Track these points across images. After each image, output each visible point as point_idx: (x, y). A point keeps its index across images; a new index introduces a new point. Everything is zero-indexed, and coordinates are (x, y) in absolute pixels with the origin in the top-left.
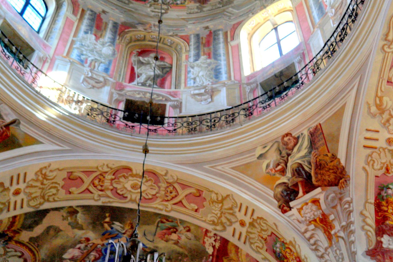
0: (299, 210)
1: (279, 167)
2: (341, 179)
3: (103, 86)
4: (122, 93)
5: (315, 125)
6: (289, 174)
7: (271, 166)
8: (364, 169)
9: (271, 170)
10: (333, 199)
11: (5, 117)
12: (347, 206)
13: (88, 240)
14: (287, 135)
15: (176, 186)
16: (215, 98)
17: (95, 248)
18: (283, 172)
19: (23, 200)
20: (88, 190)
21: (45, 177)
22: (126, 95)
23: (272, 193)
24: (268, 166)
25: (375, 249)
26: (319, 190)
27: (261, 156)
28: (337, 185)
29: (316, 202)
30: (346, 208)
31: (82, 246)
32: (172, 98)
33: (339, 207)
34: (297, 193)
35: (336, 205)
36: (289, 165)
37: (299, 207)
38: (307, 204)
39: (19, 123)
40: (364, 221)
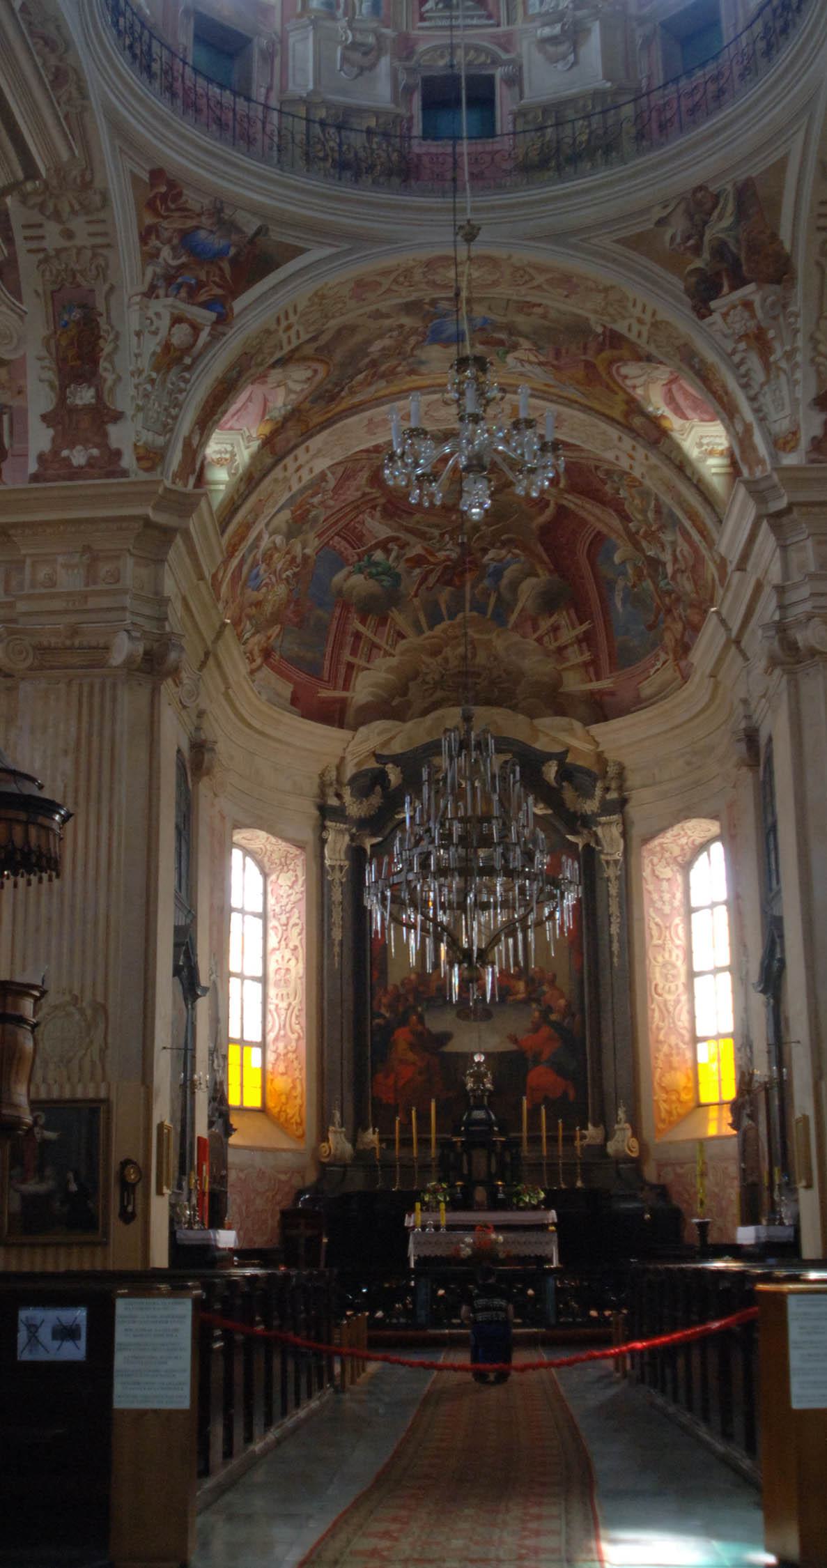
0: (725, 316)
1: (691, 242)
2: (785, 274)
3: (378, 58)
4: (412, 63)
5: (744, 177)
6: (706, 255)
7: (678, 240)
9: (679, 245)
10: (773, 305)
11: (245, 229)
12: (792, 320)
13: (402, 326)
14: (701, 188)
15: (531, 271)
16: (583, 51)
17: (414, 331)
18: (697, 250)
19: (298, 331)
20: (389, 290)
21: (323, 297)
22: (420, 66)
24: (673, 238)
26: (751, 287)
27: (661, 222)
28: (778, 282)
29: (748, 305)
30: (790, 324)
31: (395, 333)
32: (504, 56)
33: (781, 319)
34: (721, 286)
35: (778, 315)
36: (707, 238)
37: (724, 310)
38: (734, 307)
39: (267, 229)
40: (815, 349)
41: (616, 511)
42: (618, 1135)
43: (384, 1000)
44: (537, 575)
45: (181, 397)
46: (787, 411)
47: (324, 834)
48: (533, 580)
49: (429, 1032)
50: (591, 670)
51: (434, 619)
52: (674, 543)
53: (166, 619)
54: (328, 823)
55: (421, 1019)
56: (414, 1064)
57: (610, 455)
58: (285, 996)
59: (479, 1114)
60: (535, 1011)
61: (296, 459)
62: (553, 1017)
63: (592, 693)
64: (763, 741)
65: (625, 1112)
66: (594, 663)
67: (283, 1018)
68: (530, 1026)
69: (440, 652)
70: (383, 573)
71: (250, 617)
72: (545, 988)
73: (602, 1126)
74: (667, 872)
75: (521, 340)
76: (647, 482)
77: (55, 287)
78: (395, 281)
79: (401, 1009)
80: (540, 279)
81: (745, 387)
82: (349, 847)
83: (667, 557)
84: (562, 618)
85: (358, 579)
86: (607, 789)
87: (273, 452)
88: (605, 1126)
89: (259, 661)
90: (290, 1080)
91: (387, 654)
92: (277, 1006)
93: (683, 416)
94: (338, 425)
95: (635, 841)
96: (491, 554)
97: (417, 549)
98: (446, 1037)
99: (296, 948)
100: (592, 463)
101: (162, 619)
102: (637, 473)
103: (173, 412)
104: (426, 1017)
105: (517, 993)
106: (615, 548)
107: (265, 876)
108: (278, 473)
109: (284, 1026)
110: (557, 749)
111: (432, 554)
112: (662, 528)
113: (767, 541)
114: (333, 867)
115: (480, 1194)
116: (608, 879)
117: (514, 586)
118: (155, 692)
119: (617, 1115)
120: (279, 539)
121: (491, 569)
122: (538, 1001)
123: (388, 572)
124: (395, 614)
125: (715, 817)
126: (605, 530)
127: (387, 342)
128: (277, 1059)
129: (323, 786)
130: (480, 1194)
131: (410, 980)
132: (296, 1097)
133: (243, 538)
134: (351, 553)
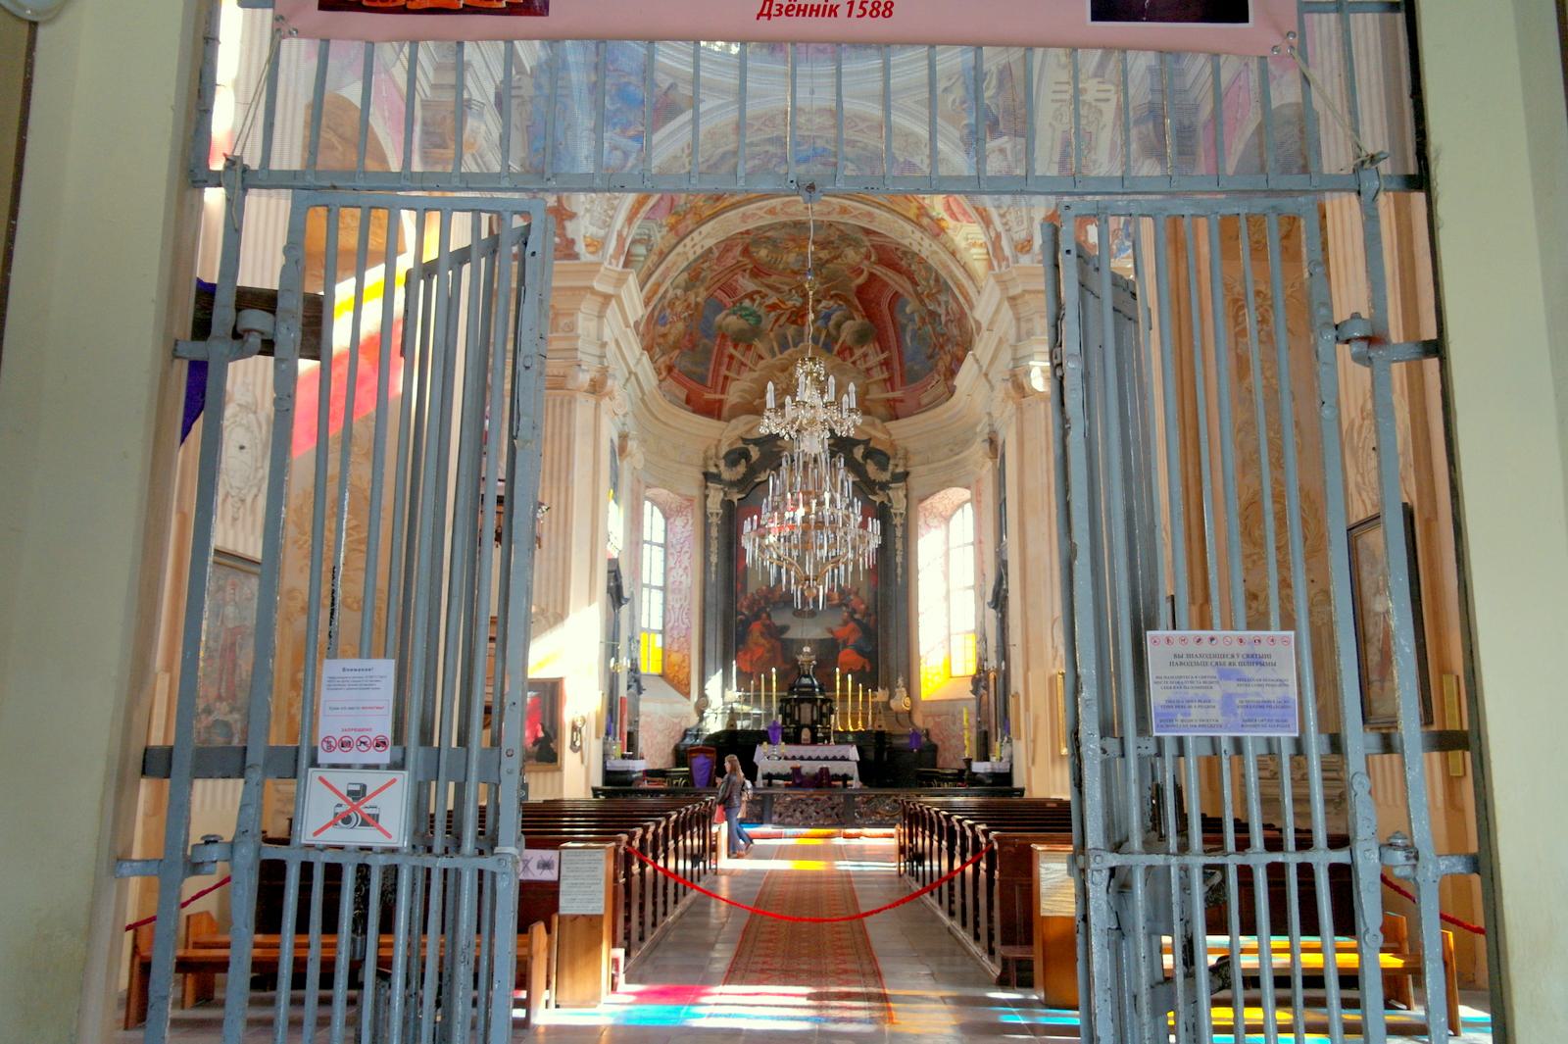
8: (1050, 124)
20: (759, 130)
23: (957, 134)
24: (954, 101)
25: (1053, 215)
26: (1006, 138)
31: (762, 157)
41: (909, 278)
44: (854, 319)
45: (616, 202)
46: (1025, 225)
47: (707, 492)
48: (850, 323)
50: (888, 384)
51: (784, 346)
52: (947, 302)
53: (605, 357)
54: (709, 484)
56: (763, 645)
57: (906, 242)
59: (806, 681)
60: (844, 613)
61: (692, 239)
62: (857, 616)
63: (888, 400)
64: (1000, 442)
66: (890, 380)
68: (840, 622)
69: (787, 369)
70: (750, 315)
71: (659, 345)
72: (852, 597)
74: (934, 522)
75: (849, 164)
76: (930, 261)
77: (529, 123)
78: (764, 124)
80: (862, 125)
81: (998, 207)
82: (723, 501)
83: (941, 311)
84: (870, 348)
85: (732, 319)
86: (897, 466)
87: (677, 234)
89: (664, 374)
91: (751, 370)
93: (957, 220)
94: (722, 217)
95: (913, 501)
96: (824, 303)
97: (773, 299)
98: (785, 629)
99: (686, 568)
100: (893, 246)
101: (602, 357)
102: (924, 255)
103: (610, 213)
104: (772, 615)
106: (907, 303)
107: (666, 518)
108: (680, 249)
110: (865, 438)
111: (783, 303)
112: (939, 292)
113: (1007, 312)
114: (712, 514)
115: (806, 734)
116: (896, 526)
117: (838, 326)
118: (597, 406)
120: (679, 292)
121: (823, 314)
122: (847, 606)
123: (753, 314)
124: (756, 342)
125: (968, 488)
126: (901, 291)
127: (756, 162)
129: (706, 459)
130: (806, 734)
133: (655, 292)
134: (727, 300)
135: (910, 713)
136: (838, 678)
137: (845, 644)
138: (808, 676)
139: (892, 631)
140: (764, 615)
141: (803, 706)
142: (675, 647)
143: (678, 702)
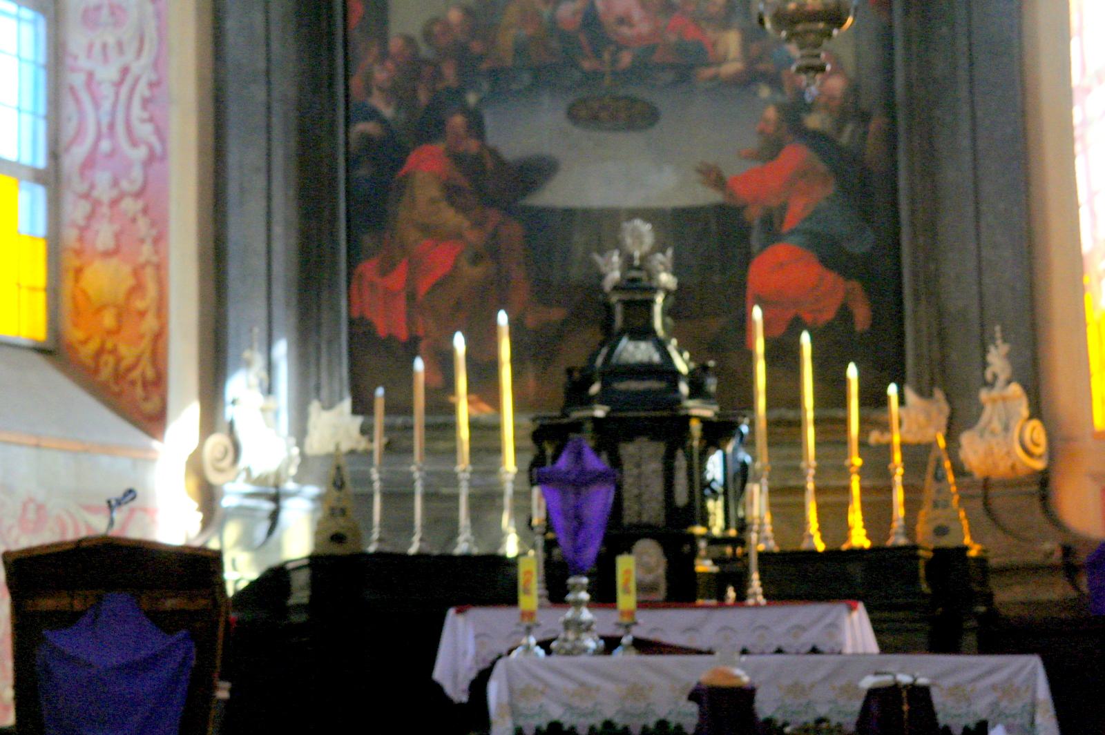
42: (991, 415)
43: (381, 75)
49: (494, 153)
55: (476, 126)
56: (458, 235)
58: (112, 53)
59: (636, 351)
62: (814, 121)
65: (1009, 356)
67: (106, 105)
68: (753, 143)
73: (939, 394)
79: (423, 97)
88: (949, 398)
90: (126, 269)
92: (90, 75)
104: (488, 120)
105: (724, 60)
109: (112, 126)
119: (985, 365)
128: (90, 217)
131: (446, 24)
132: (142, 314)
135: (1044, 481)
136: (760, 346)
137: (772, 227)
138: (643, 332)
139: (954, 174)
140: (458, 121)
141: (628, 450)
142: (104, 236)
143: (107, 449)
